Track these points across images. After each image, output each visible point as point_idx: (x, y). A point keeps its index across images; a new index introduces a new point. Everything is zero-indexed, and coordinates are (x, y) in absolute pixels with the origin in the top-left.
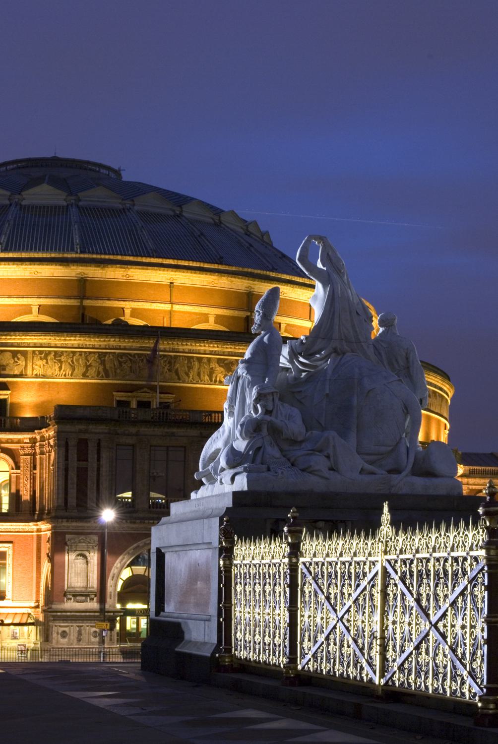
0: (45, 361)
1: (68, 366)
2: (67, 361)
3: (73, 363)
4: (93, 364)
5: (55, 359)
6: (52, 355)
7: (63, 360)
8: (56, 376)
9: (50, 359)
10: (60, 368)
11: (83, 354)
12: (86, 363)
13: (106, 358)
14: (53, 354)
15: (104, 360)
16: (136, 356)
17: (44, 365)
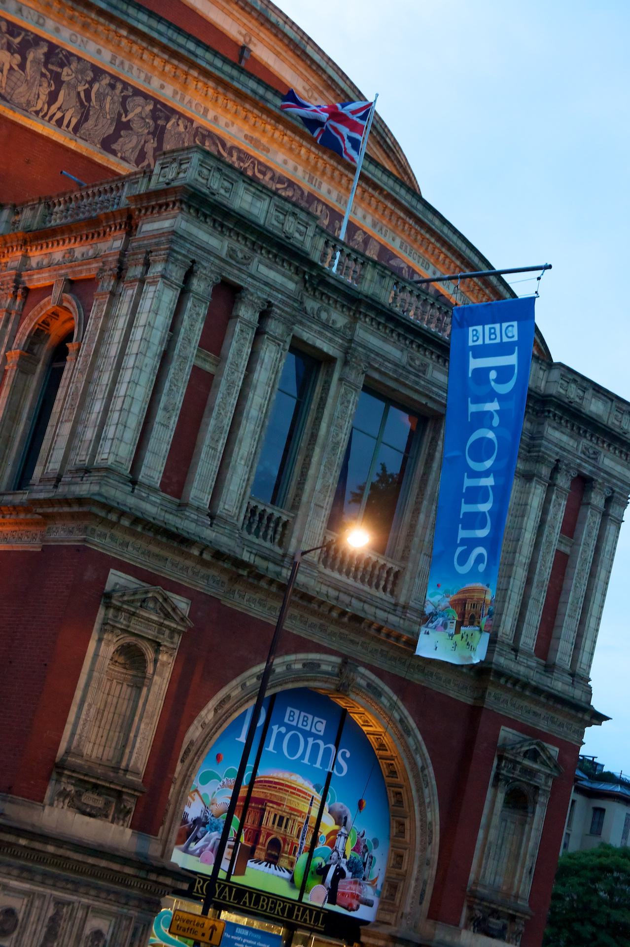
0: (18, 57)
1: (74, 101)
2: (76, 87)
3: (89, 99)
4: (134, 126)
5: (46, 66)
6: (37, 54)
7: (65, 78)
8: (37, 113)
9: (35, 61)
10: (53, 97)
11: (119, 86)
12: (120, 115)
13: (169, 125)
14: (45, 49)
15: (164, 128)
16: (235, 154)
17: (11, 68)
